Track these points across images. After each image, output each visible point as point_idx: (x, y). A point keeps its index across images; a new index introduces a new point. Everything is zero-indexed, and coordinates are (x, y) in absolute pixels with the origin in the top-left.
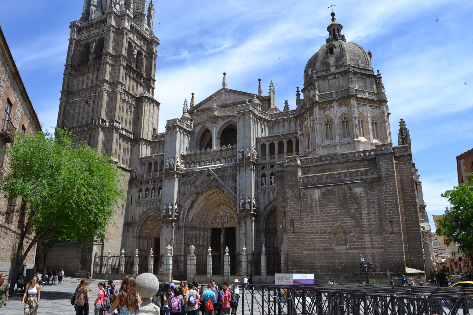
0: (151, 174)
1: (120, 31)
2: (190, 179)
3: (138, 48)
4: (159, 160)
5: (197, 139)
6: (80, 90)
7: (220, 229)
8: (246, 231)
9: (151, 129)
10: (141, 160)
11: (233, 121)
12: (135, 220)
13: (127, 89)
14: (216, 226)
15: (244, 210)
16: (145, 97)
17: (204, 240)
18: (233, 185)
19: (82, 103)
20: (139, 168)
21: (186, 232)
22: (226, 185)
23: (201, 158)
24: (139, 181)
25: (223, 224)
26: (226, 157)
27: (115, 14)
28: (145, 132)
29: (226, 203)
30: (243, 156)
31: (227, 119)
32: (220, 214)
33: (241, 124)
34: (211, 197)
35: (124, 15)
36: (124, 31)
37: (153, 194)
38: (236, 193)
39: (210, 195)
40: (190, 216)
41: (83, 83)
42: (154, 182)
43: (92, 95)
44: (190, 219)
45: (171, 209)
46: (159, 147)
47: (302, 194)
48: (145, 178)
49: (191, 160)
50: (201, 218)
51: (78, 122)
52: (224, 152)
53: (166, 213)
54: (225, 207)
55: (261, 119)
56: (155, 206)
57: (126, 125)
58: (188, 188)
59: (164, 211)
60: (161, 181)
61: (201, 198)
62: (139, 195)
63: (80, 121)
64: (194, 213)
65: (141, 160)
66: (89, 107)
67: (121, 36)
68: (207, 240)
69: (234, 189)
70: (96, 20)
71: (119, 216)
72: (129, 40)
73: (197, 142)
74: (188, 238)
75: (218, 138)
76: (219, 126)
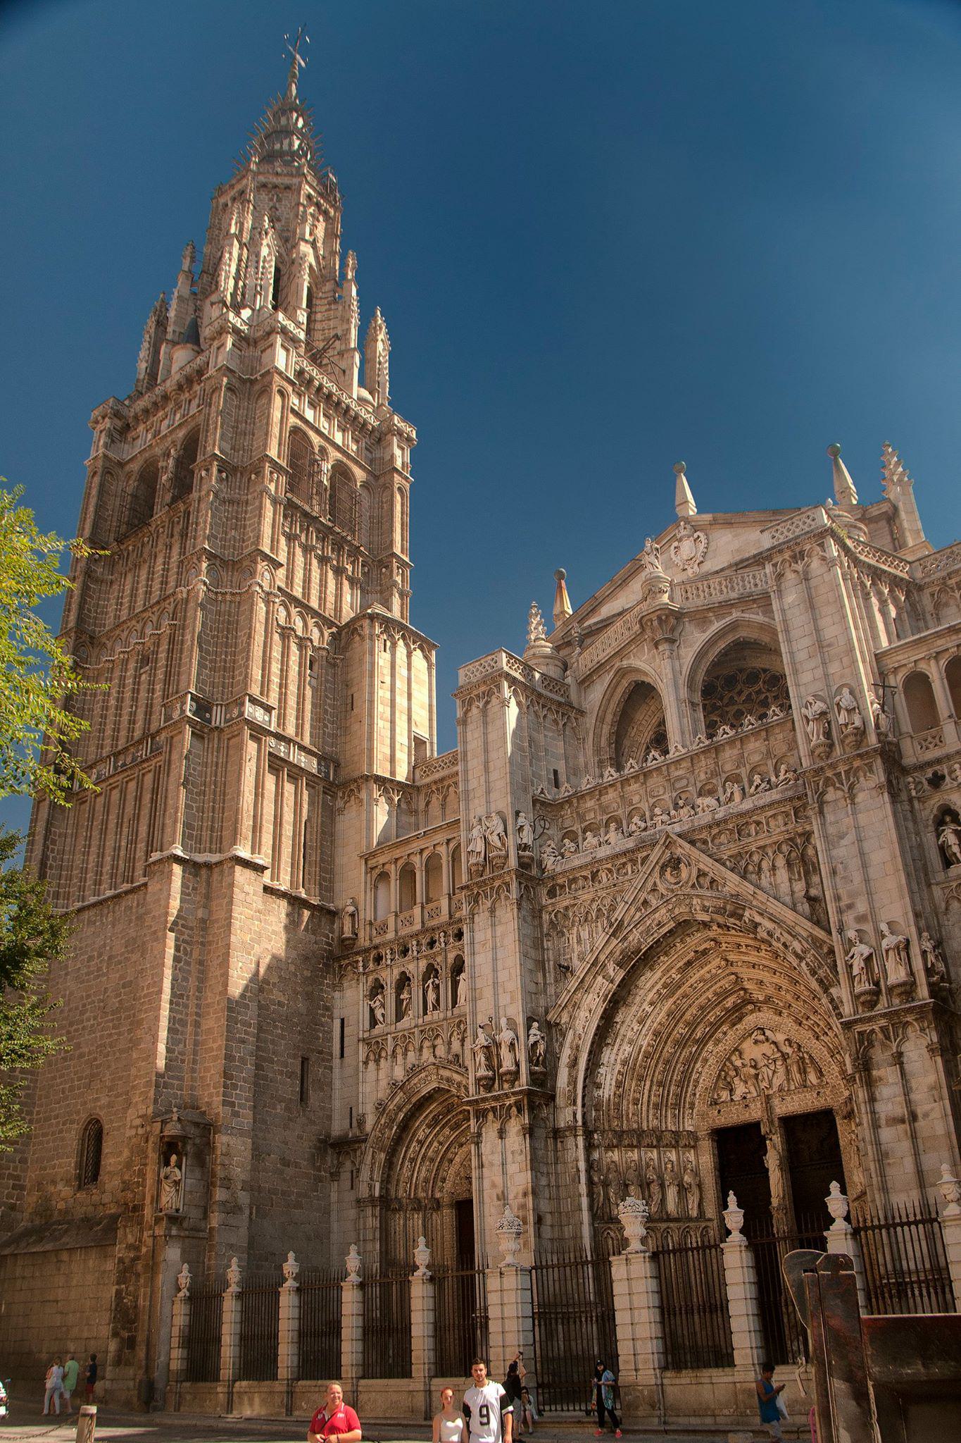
0: (417, 910)
1: (257, 387)
2: (585, 896)
3: (334, 455)
4: (442, 850)
5: (597, 736)
6: (124, 622)
7: (755, 1126)
8: (908, 1102)
9: (402, 738)
10: (372, 863)
11: (749, 624)
12: (361, 1123)
13: (298, 592)
14: (733, 1116)
15: (877, 993)
16: (372, 617)
17: (682, 1190)
18: (800, 887)
19: (132, 665)
20: (365, 900)
21: (596, 1155)
22: (762, 896)
24: (367, 950)
25: (768, 1097)
26: (744, 772)
27: (236, 331)
28: (381, 750)
29: (768, 1000)
30: (828, 734)
31: (718, 617)
32: (747, 1056)
33: (792, 597)
34: (696, 975)
35: (269, 334)
36: (271, 383)
37: (431, 996)
38: (820, 921)
39: (689, 963)
40: (608, 1077)
41: (133, 595)
42: (432, 944)
43: (165, 629)
44: (607, 1091)
45: (512, 1046)
46: (443, 806)
48: (390, 935)
49: (582, 818)
50: (660, 1084)
51: (115, 739)
52: (729, 754)
53: (489, 1067)
54: (764, 1017)
55: (876, 574)
56: (441, 1051)
57: (299, 728)
58: (579, 941)
59: (481, 1058)
60: (459, 935)
61: (651, 981)
62: (372, 1010)
63: (123, 733)
64: (625, 1063)
65: (372, 863)
66: (153, 674)
67: (264, 401)
68: (700, 1186)
69: (806, 907)
70: (176, 377)
71: (287, 1109)
72: (293, 420)
73: (598, 751)
74: (606, 1184)
75: (693, 704)
76: (688, 654)
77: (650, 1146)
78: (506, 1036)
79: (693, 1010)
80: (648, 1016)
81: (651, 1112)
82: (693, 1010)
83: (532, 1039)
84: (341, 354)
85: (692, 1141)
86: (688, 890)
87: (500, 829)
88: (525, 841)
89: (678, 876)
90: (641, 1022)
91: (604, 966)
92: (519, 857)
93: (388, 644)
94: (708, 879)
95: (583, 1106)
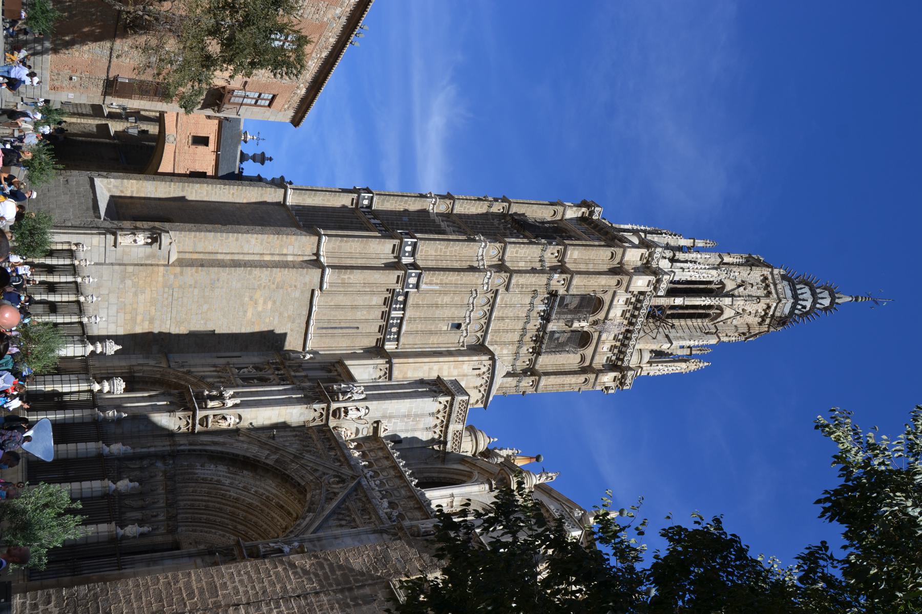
10: (337, 365)
21: (159, 464)
23: (383, 470)
34: (276, 515)
39: (282, 507)
47: (367, 591)
48: (293, 374)
49: (370, 451)
61: (269, 487)
64: (219, 481)
65: (337, 365)
74: (142, 469)
77: (167, 499)
78: (230, 403)
79: (254, 519)
80: (248, 491)
81: (189, 503)
82: (254, 519)
83: (228, 417)
84: (667, 336)
85: (172, 531)
86: (324, 490)
87: (356, 397)
88: (350, 412)
89: (333, 483)
90: (245, 489)
91: (275, 453)
92: (339, 409)
93: (477, 372)
94: (331, 496)
95: (189, 450)
